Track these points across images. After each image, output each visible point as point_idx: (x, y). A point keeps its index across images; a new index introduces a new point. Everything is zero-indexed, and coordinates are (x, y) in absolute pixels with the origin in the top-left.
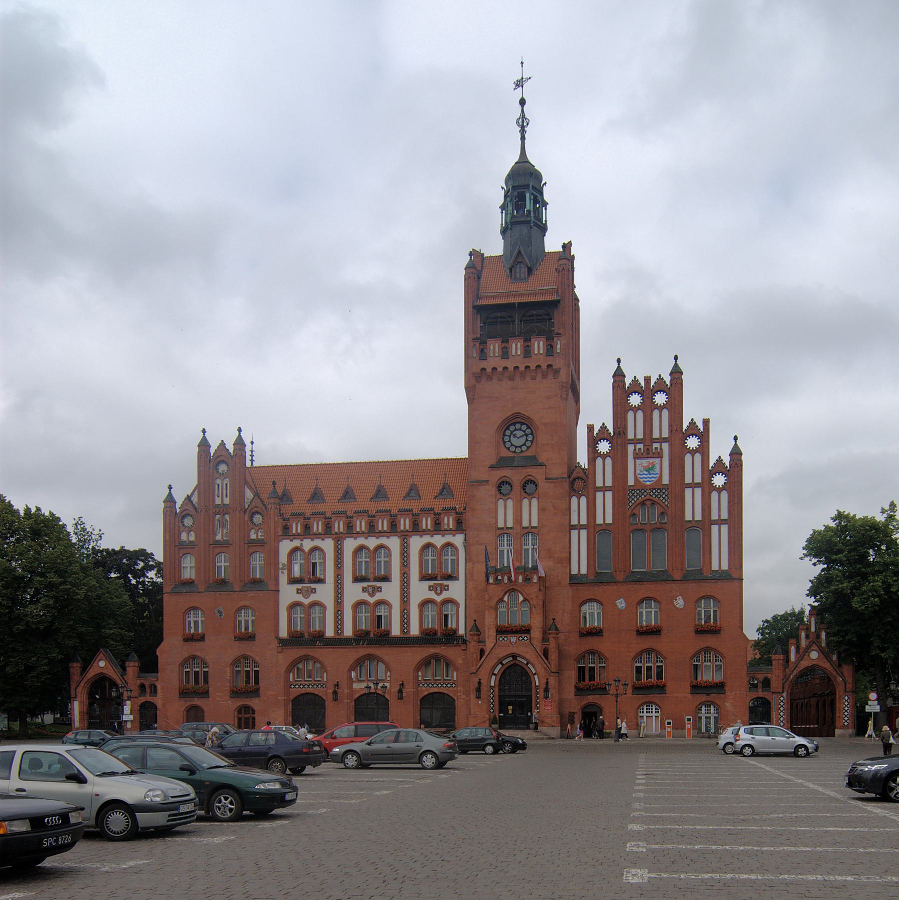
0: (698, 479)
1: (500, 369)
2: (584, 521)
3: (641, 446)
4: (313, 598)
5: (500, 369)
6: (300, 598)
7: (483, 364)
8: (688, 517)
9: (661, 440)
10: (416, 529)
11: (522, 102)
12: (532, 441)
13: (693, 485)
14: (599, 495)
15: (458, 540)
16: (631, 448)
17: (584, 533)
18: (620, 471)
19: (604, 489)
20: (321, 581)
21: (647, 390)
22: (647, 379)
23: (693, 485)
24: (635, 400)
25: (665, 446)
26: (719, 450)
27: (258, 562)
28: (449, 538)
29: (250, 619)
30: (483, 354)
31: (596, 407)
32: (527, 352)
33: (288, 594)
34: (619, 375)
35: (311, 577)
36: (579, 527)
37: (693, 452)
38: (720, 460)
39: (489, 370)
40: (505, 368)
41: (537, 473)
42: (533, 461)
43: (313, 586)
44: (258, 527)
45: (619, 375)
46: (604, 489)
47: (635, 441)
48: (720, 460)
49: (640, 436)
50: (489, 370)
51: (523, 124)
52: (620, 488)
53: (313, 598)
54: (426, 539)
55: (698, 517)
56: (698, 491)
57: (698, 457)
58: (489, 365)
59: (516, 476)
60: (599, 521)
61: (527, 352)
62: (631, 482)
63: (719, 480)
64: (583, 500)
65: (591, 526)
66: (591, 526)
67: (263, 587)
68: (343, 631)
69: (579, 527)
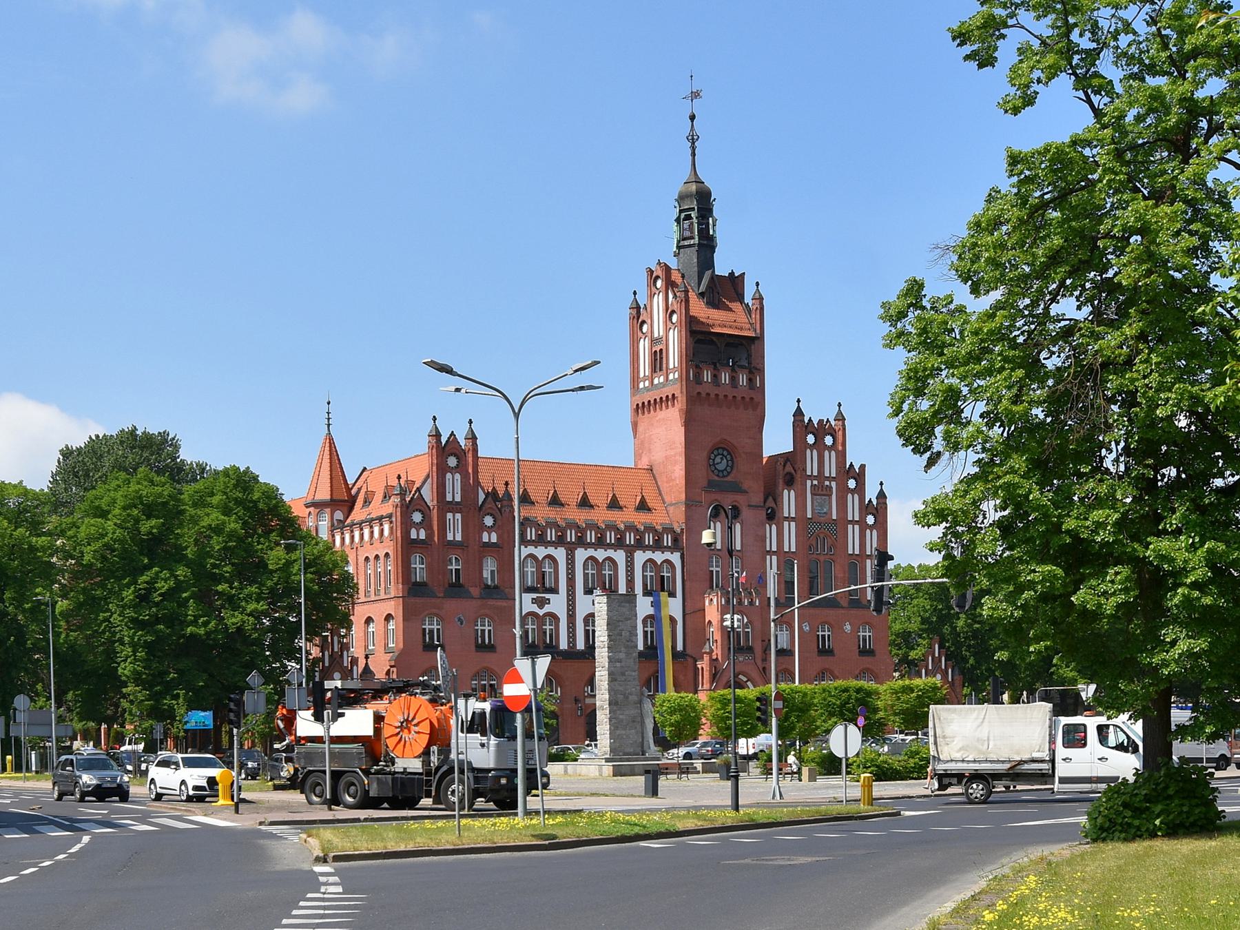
0: (857, 518)
1: (712, 396)
2: (774, 549)
3: (815, 482)
4: (547, 609)
5: (712, 396)
6: (535, 608)
7: (699, 389)
8: (850, 552)
9: (830, 479)
10: (640, 545)
11: (692, 118)
12: (732, 468)
13: (853, 522)
14: (786, 524)
15: (675, 558)
16: (809, 482)
17: (774, 558)
18: (801, 505)
19: (788, 519)
20: (554, 591)
21: (822, 429)
22: (821, 421)
23: (853, 522)
24: (811, 439)
25: (834, 484)
26: (871, 494)
27: (489, 568)
28: (668, 555)
29: (487, 628)
30: (698, 379)
31: (777, 439)
32: (734, 379)
33: (525, 603)
34: (799, 413)
35: (542, 587)
36: (770, 553)
37: (853, 491)
38: (870, 501)
39: (704, 395)
40: (717, 395)
41: (740, 500)
42: (736, 488)
43: (547, 596)
44: (490, 530)
45: (799, 413)
46: (788, 519)
47: (811, 477)
48: (870, 501)
49: (815, 473)
50: (704, 395)
51: (693, 140)
52: (800, 519)
53: (547, 609)
54: (649, 554)
55: (857, 552)
56: (857, 527)
57: (856, 496)
58: (703, 389)
59: (727, 501)
60: (786, 549)
61: (734, 379)
62: (809, 516)
63: (870, 520)
64: (774, 527)
65: (779, 552)
66: (779, 552)
67: (499, 592)
68: (575, 645)
69: (770, 553)
